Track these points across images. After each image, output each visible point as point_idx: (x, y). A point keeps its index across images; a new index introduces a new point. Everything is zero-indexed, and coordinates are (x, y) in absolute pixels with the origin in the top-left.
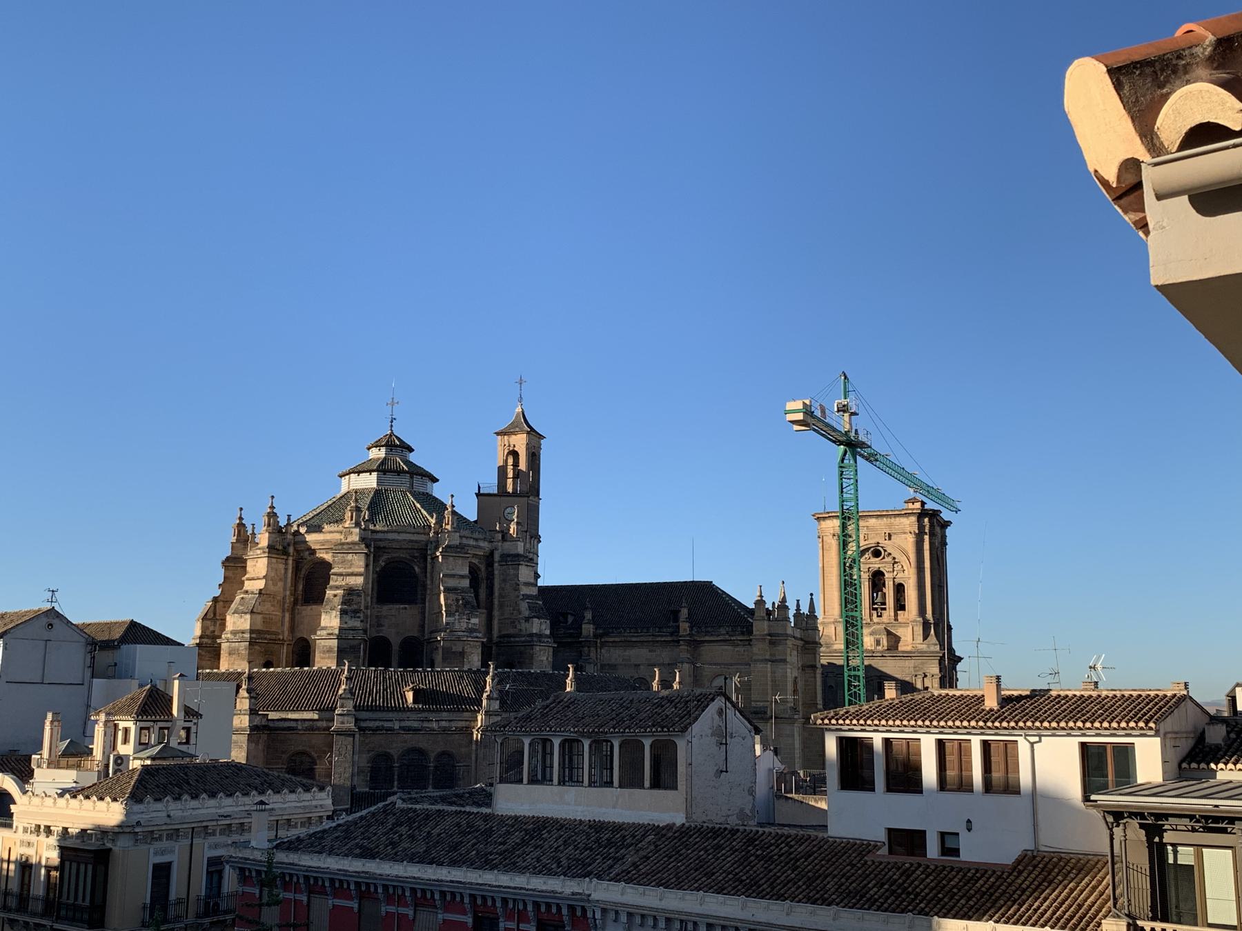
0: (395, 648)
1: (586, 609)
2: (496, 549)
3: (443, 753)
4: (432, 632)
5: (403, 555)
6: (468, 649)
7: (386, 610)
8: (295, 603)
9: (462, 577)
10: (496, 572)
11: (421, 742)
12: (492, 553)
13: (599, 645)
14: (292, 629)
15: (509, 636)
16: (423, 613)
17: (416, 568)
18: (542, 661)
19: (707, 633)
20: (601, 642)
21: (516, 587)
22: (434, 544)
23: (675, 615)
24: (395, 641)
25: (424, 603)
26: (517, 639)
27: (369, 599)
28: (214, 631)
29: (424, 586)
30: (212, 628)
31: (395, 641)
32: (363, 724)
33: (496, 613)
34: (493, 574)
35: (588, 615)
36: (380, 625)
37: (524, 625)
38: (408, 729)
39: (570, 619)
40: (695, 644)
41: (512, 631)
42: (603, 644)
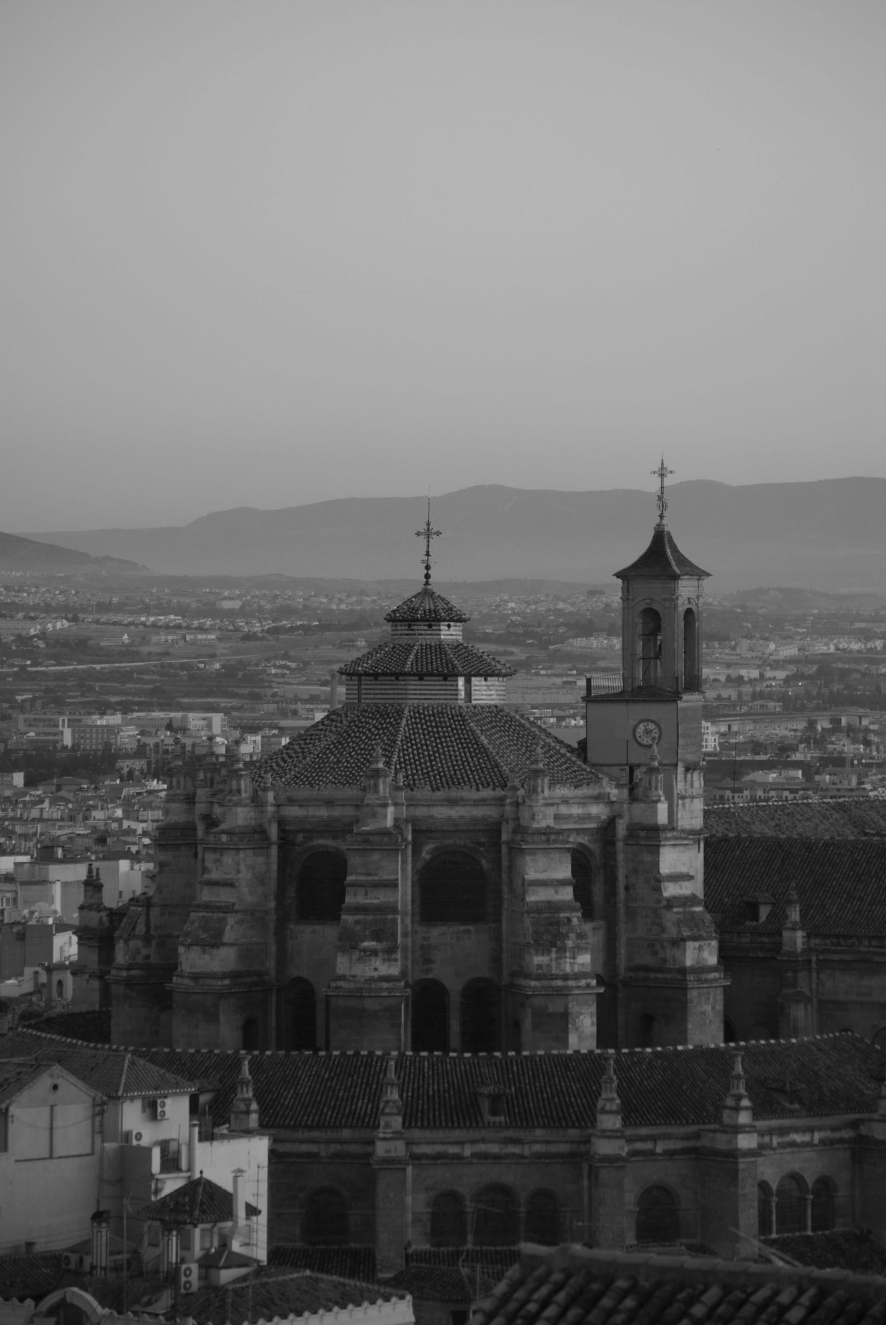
0: (455, 998)
1: (790, 902)
2: (620, 816)
4: (513, 974)
6: (573, 1007)
7: (437, 933)
9: (563, 883)
10: (620, 857)
11: (507, 1176)
12: (610, 825)
13: (814, 965)
15: (647, 969)
16: (497, 937)
17: (484, 862)
18: (704, 1013)
20: (819, 962)
21: (656, 881)
22: (511, 825)
24: (454, 986)
25: (499, 921)
26: (660, 976)
27: (408, 920)
28: (147, 957)
30: (144, 952)
31: (454, 986)
32: (418, 1150)
33: (622, 928)
34: (615, 860)
35: (795, 914)
36: (428, 961)
38: (484, 1156)
39: (764, 912)
41: (648, 960)
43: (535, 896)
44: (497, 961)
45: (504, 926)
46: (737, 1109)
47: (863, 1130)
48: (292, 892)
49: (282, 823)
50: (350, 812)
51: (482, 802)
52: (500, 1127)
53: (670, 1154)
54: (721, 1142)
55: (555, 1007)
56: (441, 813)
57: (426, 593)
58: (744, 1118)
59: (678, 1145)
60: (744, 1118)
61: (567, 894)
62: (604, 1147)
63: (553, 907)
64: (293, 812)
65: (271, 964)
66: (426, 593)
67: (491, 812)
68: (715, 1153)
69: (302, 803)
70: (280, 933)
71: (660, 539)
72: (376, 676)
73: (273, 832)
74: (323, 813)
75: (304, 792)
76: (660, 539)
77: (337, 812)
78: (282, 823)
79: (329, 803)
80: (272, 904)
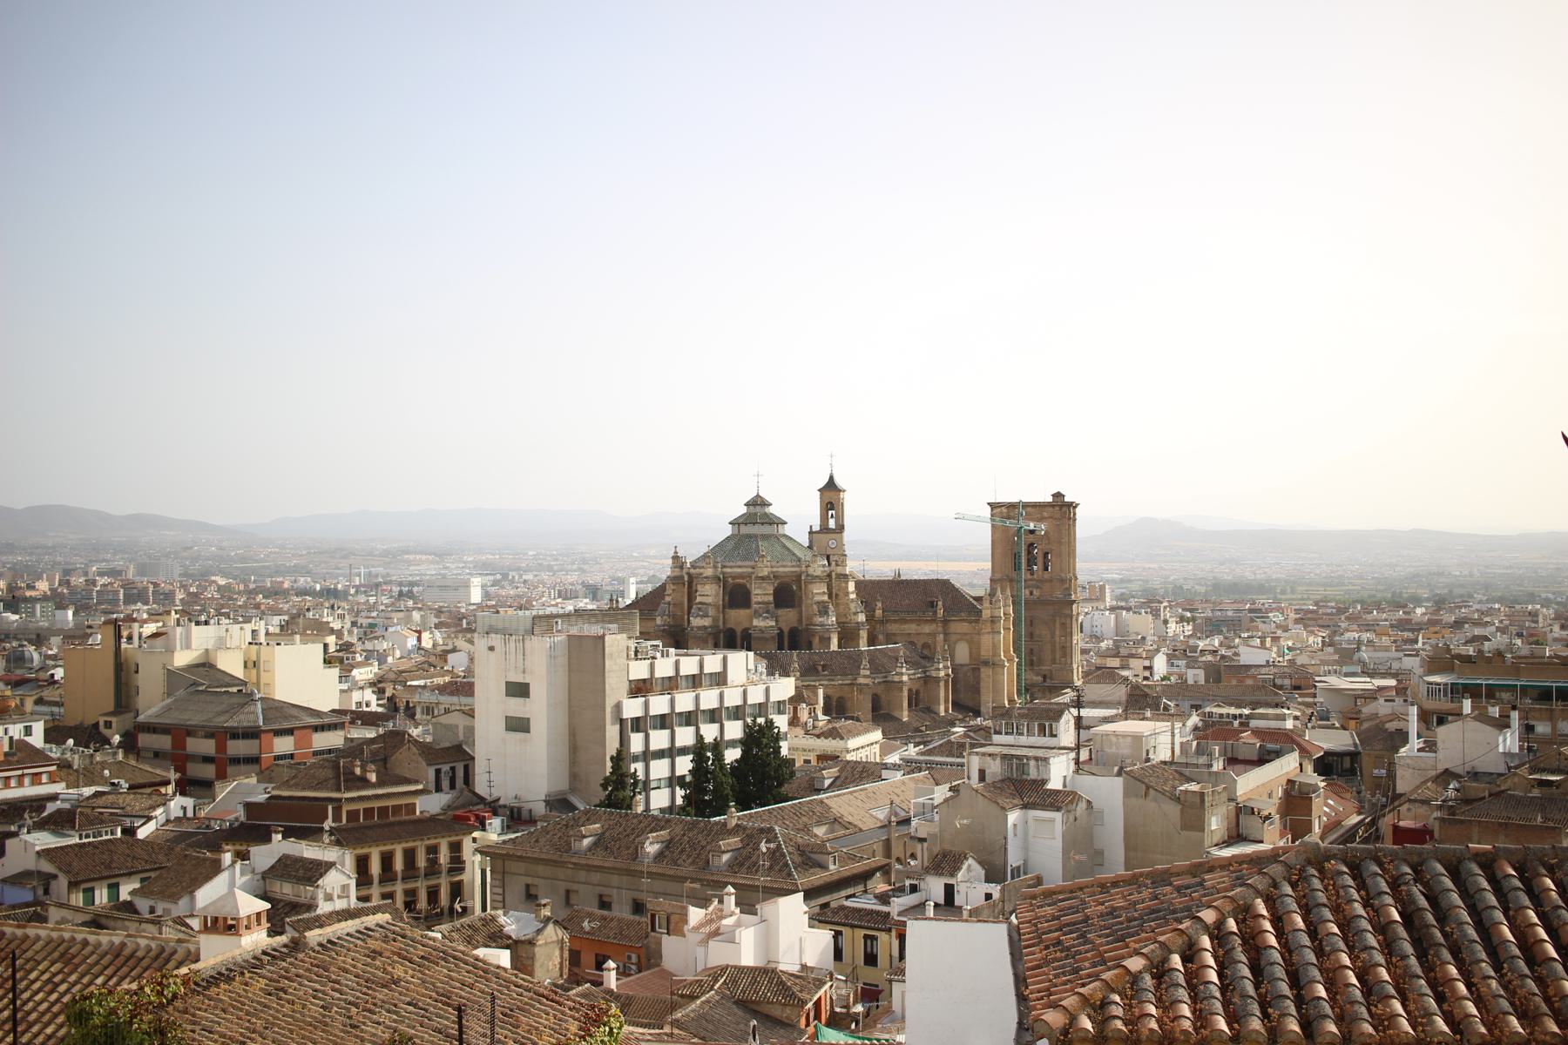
3: (840, 698)
5: (787, 580)
8: (724, 607)
14: (724, 623)
16: (800, 613)
19: (953, 615)
23: (932, 605)
24: (786, 630)
25: (800, 606)
29: (801, 597)
31: (786, 630)
37: (853, 617)
40: (945, 622)
41: (845, 620)
42: (887, 621)
43: (817, 598)
44: (800, 620)
45: (804, 609)
46: (902, 667)
47: (928, 674)
48: (727, 598)
49: (723, 573)
50: (750, 570)
51: (793, 566)
52: (826, 675)
53: (879, 683)
54: (896, 679)
55: (826, 636)
56: (781, 569)
57: (758, 496)
58: (904, 670)
59: (881, 680)
60: (904, 670)
61: (826, 598)
62: (861, 680)
63: (823, 602)
64: (725, 570)
65: (721, 623)
66: (758, 496)
67: (797, 569)
68: (895, 682)
69: (731, 567)
70: (723, 612)
71: (831, 478)
72: (746, 524)
73: (686, 578)
74: (739, 570)
75: (731, 564)
76: (831, 478)
77: (744, 570)
78: (688, 574)
79: (740, 567)
80: (721, 603)
